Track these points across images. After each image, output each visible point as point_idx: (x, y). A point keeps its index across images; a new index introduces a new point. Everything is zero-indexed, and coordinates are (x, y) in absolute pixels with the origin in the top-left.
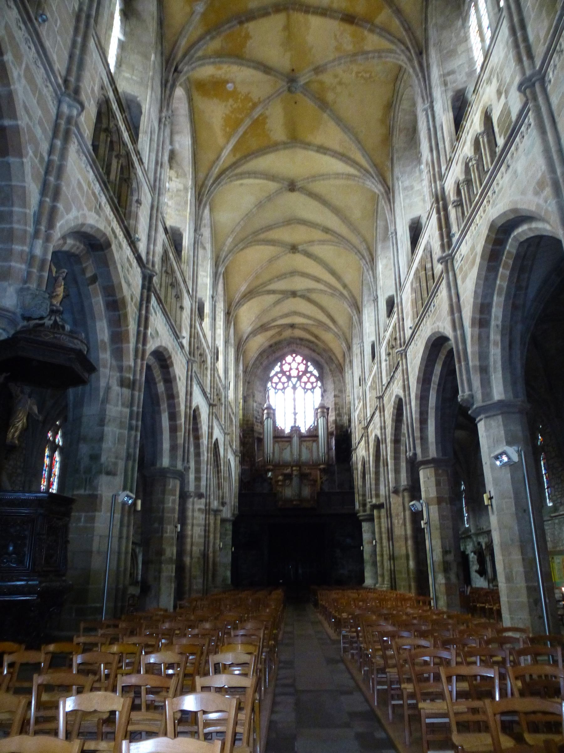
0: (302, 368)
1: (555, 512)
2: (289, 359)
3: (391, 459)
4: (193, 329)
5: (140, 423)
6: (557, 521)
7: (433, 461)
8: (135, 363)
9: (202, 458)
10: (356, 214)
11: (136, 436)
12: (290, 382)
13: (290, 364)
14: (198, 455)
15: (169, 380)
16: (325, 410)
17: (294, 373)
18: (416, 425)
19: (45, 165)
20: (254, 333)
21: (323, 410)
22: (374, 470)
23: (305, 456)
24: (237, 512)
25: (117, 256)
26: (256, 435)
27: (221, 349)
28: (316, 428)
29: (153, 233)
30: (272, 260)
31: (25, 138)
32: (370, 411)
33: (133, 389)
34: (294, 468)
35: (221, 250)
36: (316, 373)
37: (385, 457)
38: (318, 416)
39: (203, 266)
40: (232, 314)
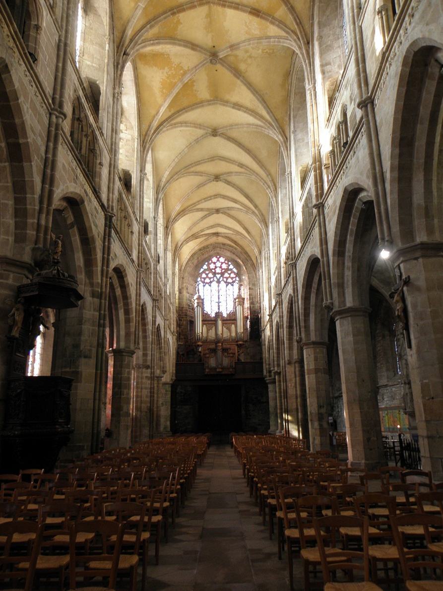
0: (224, 266)
2: (214, 260)
3: (286, 340)
4: (140, 247)
7: (314, 343)
8: (102, 280)
9: (148, 340)
10: (263, 154)
12: (215, 278)
13: (215, 263)
14: (145, 337)
15: (124, 286)
18: (302, 318)
19: (44, 161)
21: (240, 300)
23: (226, 335)
24: (174, 378)
25: (88, 208)
26: (188, 319)
27: (161, 255)
30: (200, 186)
31: (32, 149)
33: (101, 299)
35: (161, 181)
37: (282, 338)
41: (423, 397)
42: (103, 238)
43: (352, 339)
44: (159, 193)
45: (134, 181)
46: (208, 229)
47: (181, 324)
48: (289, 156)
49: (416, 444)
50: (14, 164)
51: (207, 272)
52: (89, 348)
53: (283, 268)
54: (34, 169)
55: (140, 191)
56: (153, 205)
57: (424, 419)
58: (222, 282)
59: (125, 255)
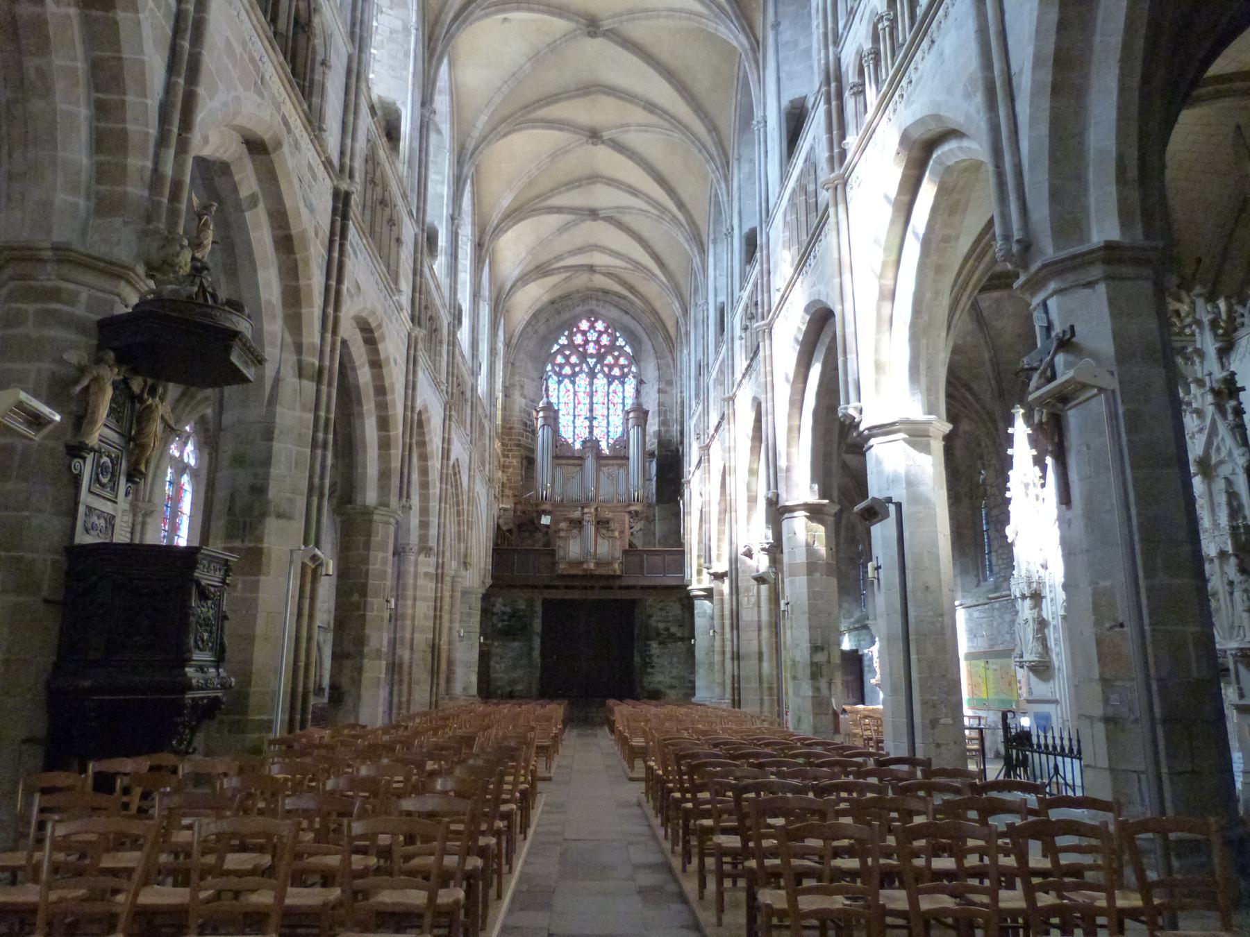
0: (605, 340)
1: (995, 592)
2: (584, 325)
4: (418, 278)
5: (331, 437)
6: (997, 605)
8: (323, 338)
11: (324, 458)
13: (584, 333)
14: (425, 485)
17: (591, 349)
19: (172, 18)
20: (524, 279)
21: (641, 414)
23: (606, 491)
24: (489, 581)
25: (291, 163)
27: (466, 305)
28: (626, 446)
29: (351, 118)
30: (556, 155)
33: (319, 382)
36: (628, 349)
39: (435, 163)
40: (486, 245)
41: (1098, 623)
42: (327, 242)
43: (905, 491)
44: (463, 164)
45: (406, 127)
46: (572, 256)
48: (761, 82)
49: (1042, 735)
50: (94, 13)
51: (567, 353)
52: (288, 495)
53: (741, 338)
54: (147, 32)
55: (420, 151)
56: (449, 188)
57: (1097, 676)
58: (600, 376)
59: (381, 291)
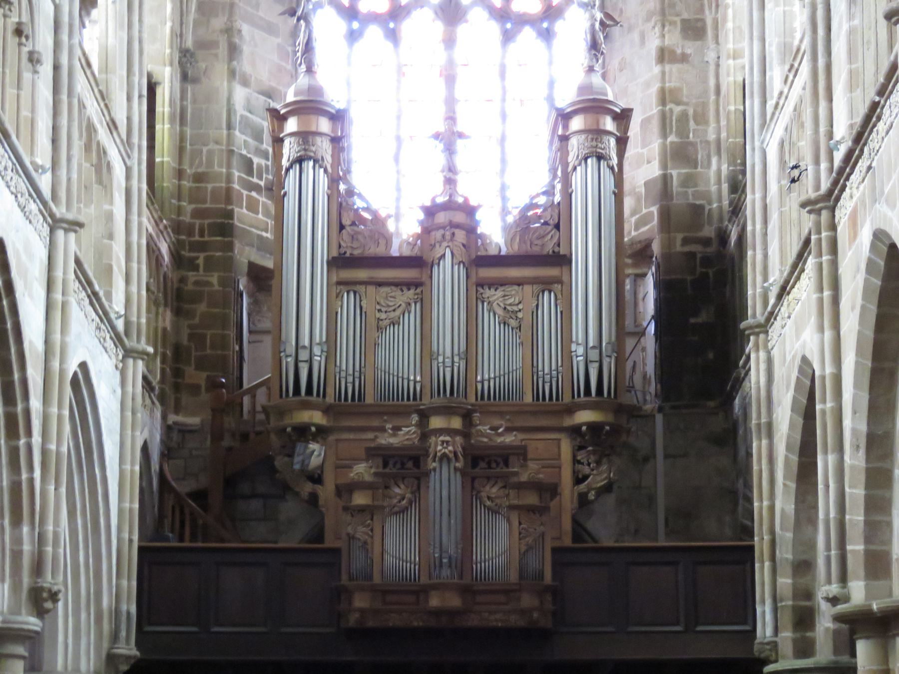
16: (609, 124)
22: (863, 427)
24: (128, 649)
32: (851, 115)
34: (436, 422)
38: (572, 159)
47: (190, 287)
